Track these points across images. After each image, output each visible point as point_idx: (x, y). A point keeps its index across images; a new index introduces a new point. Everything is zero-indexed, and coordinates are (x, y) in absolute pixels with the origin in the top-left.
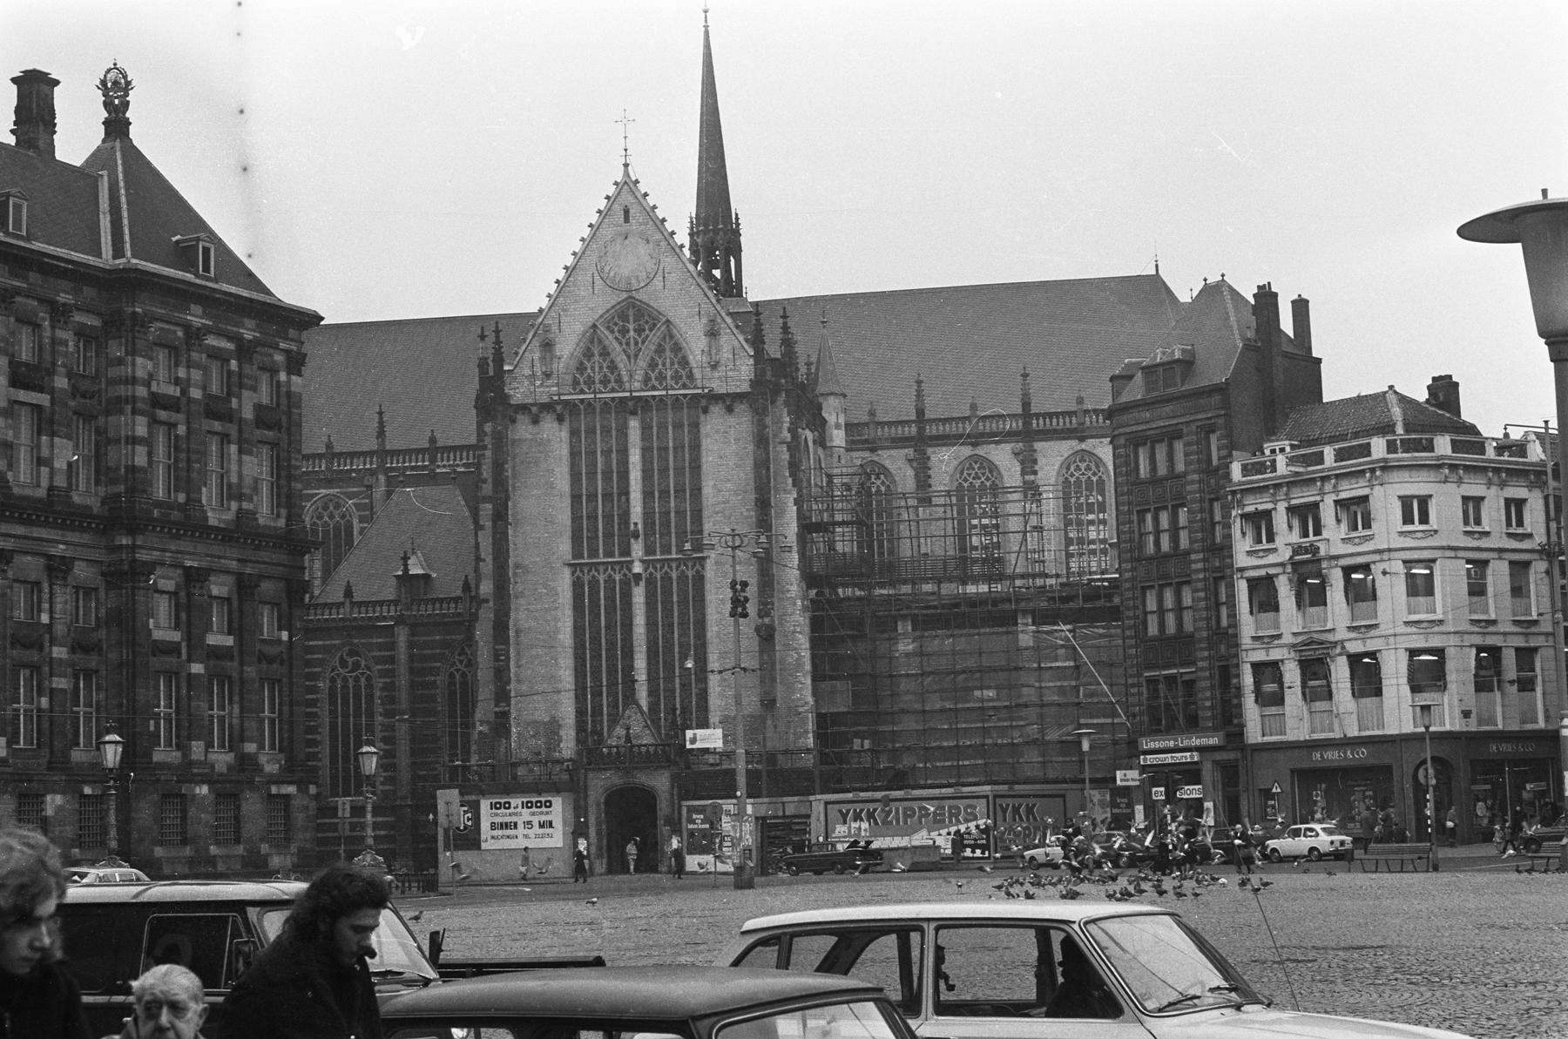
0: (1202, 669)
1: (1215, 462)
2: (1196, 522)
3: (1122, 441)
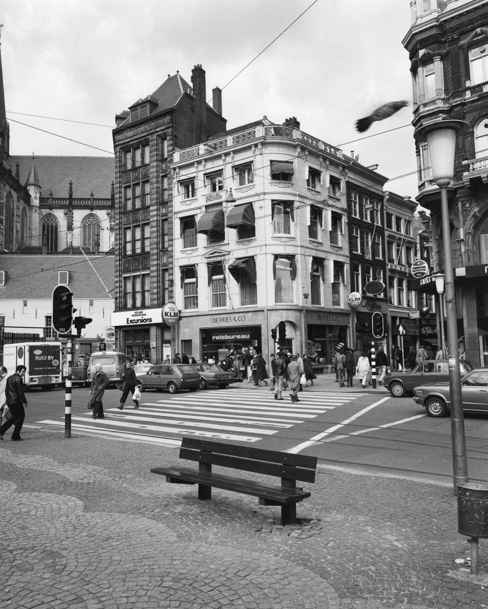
0: (153, 272)
1: (166, 156)
2: (154, 189)
3: (118, 148)
